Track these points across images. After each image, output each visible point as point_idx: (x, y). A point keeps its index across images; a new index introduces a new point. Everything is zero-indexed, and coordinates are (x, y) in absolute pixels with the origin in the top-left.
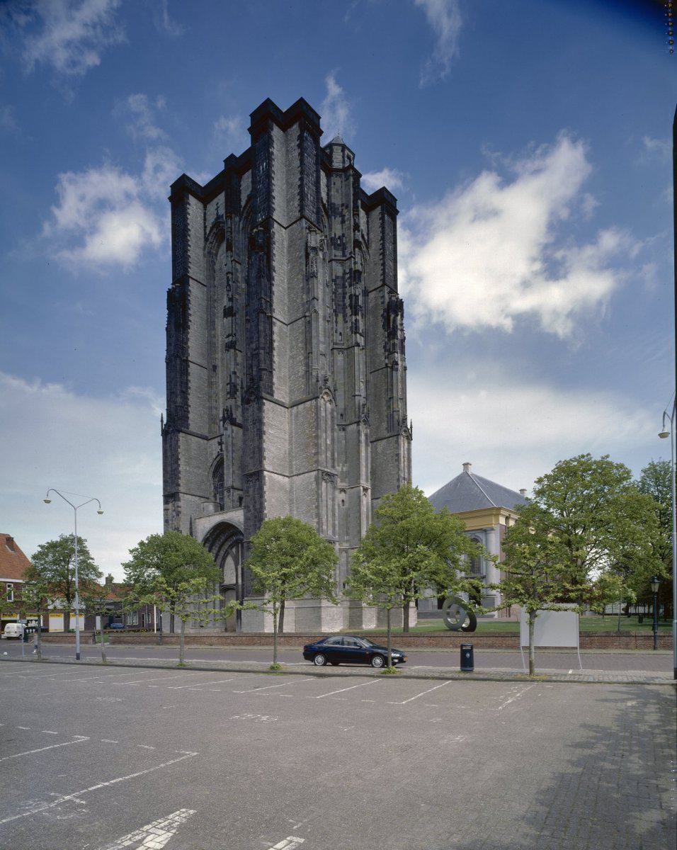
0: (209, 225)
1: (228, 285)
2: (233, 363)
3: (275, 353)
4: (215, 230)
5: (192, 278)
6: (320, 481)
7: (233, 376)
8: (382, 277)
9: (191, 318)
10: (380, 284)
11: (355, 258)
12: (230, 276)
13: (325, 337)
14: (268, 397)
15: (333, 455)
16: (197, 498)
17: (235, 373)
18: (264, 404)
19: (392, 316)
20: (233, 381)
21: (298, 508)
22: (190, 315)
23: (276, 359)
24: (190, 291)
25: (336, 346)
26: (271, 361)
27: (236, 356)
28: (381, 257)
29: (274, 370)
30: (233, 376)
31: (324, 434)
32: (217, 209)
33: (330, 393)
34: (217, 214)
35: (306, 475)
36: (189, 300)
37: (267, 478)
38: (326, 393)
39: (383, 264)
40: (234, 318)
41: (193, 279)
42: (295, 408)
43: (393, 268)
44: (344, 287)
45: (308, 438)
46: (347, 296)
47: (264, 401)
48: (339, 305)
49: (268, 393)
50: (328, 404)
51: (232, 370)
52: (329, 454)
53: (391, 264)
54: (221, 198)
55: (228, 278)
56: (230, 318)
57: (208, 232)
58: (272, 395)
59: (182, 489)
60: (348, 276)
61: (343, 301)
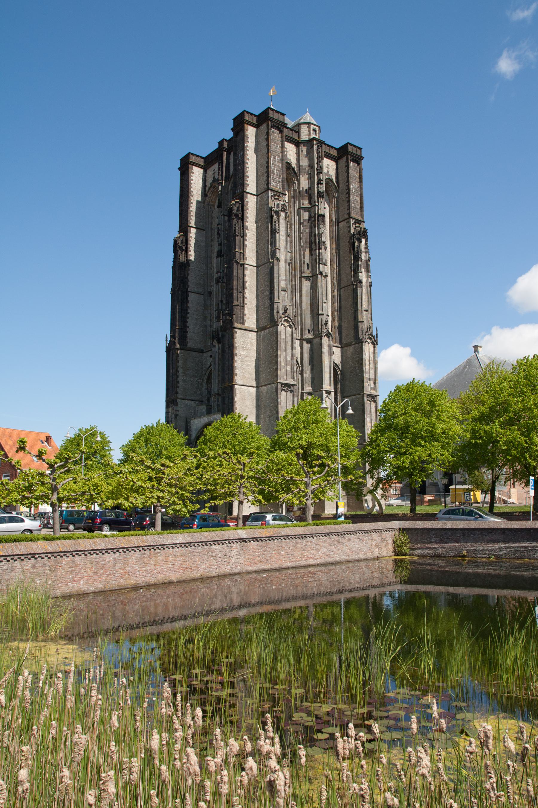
0: (208, 184)
1: (218, 233)
2: (220, 294)
3: (246, 291)
4: (212, 189)
6: (279, 391)
7: (220, 304)
8: (348, 212)
10: (347, 216)
11: (318, 206)
12: (220, 226)
13: (286, 275)
14: (239, 326)
15: (292, 368)
16: (193, 402)
17: (222, 301)
18: (236, 332)
19: (357, 244)
20: (220, 308)
21: (264, 413)
26: (244, 297)
27: (222, 287)
28: (347, 196)
29: (246, 304)
30: (220, 304)
31: (284, 353)
32: (214, 174)
33: (289, 320)
34: (214, 177)
35: (270, 386)
37: (237, 391)
38: (285, 321)
39: (349, 201)
40: (222, 258)
42: (263, 332)
43: (359, 201)
45: (271, 357)
46: (313, 235)
47: (236, 330)
48: (306, 242)
49: (240, 323)
50: (288, 329)
51: (220, 299)
52: (289, 368)
53: (358, 199)
54: (216, 166)
55: (218, 228)
56: (219, 259)
57: (207, 189)
58: (243, 324)
59: (179, 396)
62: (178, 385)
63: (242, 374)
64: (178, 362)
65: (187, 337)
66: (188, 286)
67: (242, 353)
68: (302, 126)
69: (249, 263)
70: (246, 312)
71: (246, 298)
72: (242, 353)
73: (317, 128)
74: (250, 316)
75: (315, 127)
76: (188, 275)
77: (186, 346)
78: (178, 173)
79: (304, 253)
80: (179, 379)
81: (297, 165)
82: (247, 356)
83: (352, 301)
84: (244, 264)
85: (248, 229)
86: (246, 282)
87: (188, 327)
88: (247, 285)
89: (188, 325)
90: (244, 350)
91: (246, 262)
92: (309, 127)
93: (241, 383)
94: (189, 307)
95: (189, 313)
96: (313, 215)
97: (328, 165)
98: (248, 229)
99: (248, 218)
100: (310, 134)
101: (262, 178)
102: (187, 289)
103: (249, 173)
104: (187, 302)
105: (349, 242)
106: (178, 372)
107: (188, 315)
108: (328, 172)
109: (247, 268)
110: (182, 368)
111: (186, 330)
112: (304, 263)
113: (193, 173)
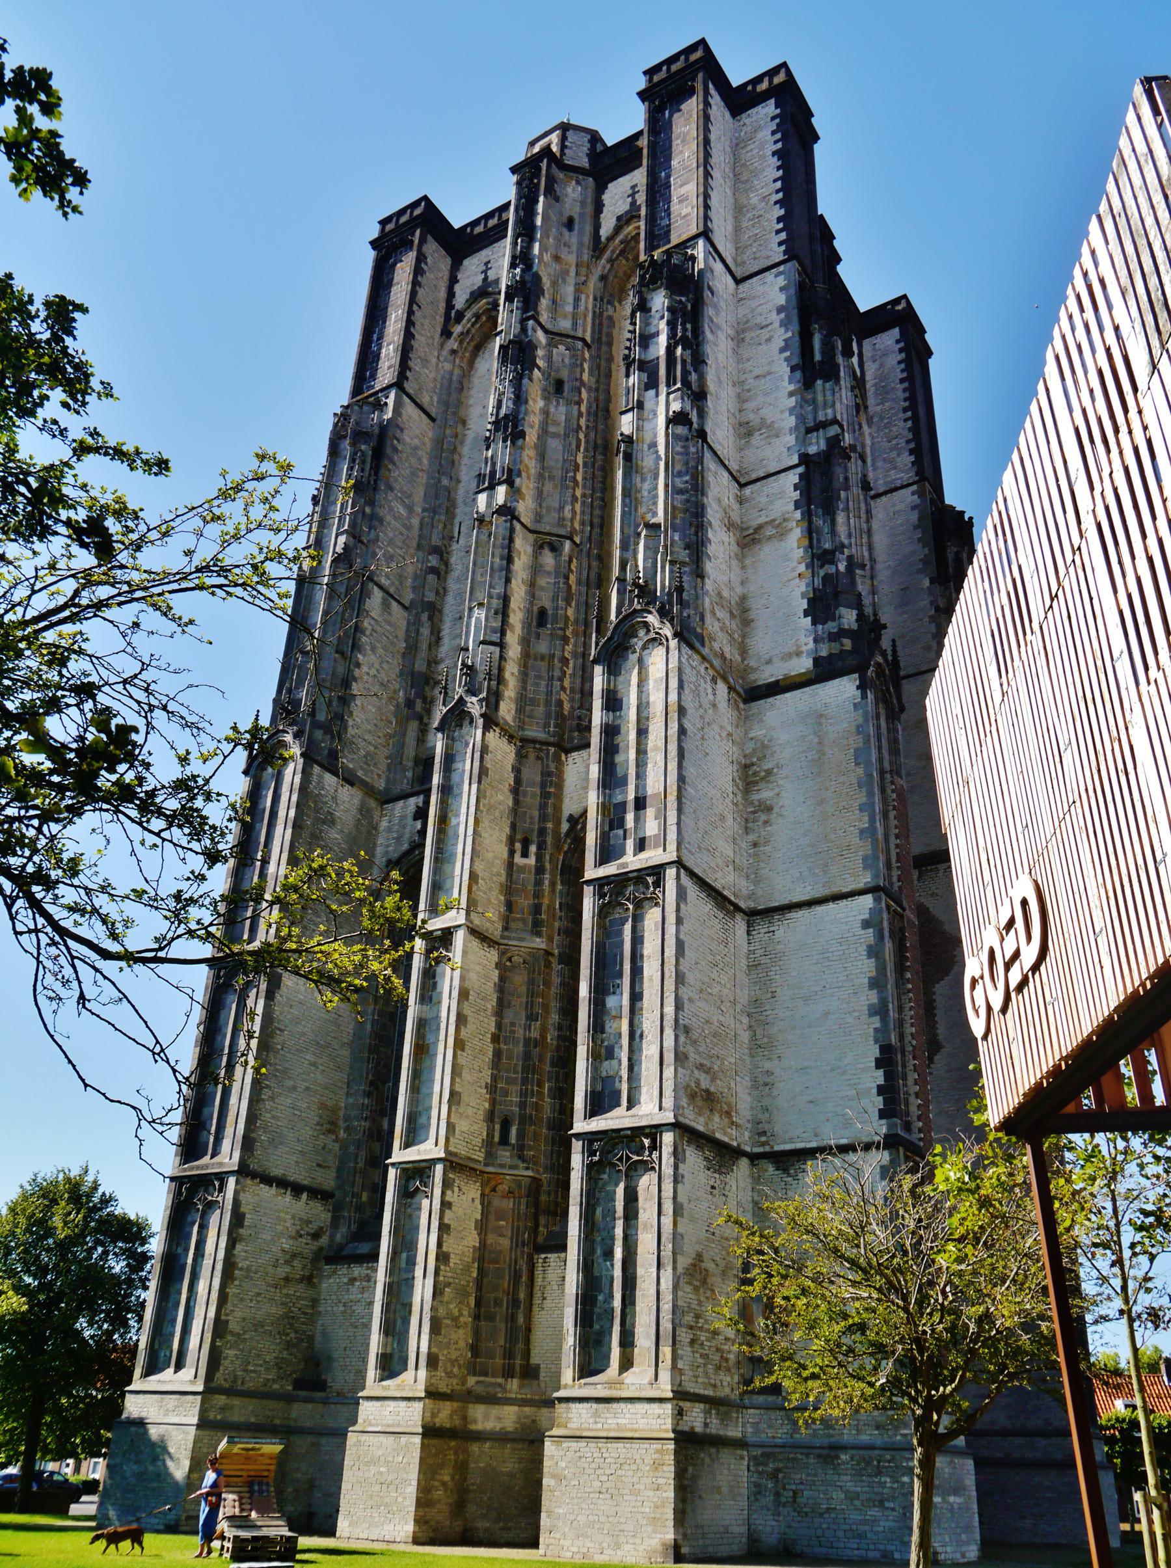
75: (546, 140)
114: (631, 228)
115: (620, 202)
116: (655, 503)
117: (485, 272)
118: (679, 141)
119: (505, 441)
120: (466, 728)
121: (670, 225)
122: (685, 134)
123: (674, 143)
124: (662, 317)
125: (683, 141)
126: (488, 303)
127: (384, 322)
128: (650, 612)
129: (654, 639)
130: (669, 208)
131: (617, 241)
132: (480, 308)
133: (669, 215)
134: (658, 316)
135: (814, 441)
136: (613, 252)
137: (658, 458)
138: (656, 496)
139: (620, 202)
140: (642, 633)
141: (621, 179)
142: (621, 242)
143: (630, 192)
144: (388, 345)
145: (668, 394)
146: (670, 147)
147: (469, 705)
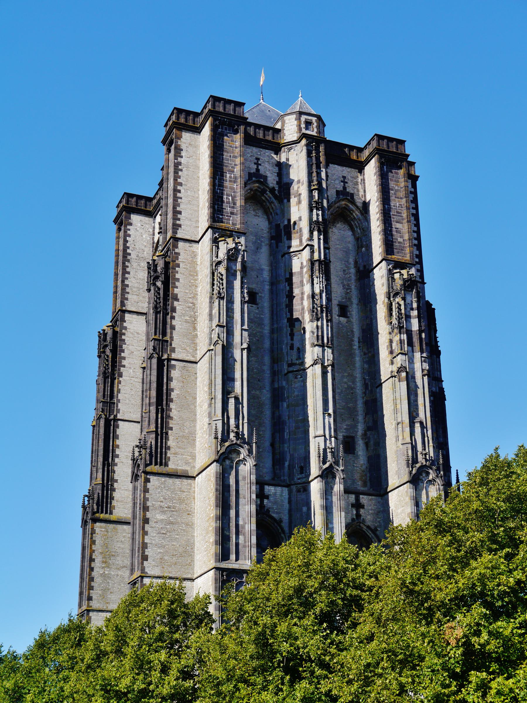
3: (172, 405)
5: (130, 312)
9: (124, 362)
22: (124, 358)
23: (174, 413)
24: (126, 328)
25: (291, 369)
29: (171, 429)
36: (124, 340)
41: (130, 312)
44: (302, 285)
46: (305, 297)
58: (166, 465)
60: (305, 270)
61: (302, 303)
62: (93, 584)
63: (159, 556)
64: (93, 542)
65: (112, 498)
66: (118, 411)
67: (160, 517)
68: (287, 118)
69: (180, 357)
70: (170, 443)
71: (172, 418)
72: (159, 517)
73: (314, 119)
74: (178, 450)
75: (310, 118)
76: (119, 391)
77: (111, 513)
78: (115, 227)
79: (292, 330)
80: (94, 574)
81: (278, 183)
82: (172, 523)
83: (393, 408)
84: (169, 360)
85: (177, 300)
86: (172, 390)
87: (116, 481)
88: (173, 395)
89: (116, 477)
90: (163, 512)
91: (174, 356)
92: (299, 119)
93: (157, 575)
94: (118, 446)
95: (117, 456)
96: (305, 263)
97: (344, 177)
98: (177, 300)
99: (178, 280)
100: (300, 129)
101: (203, 212)
102: (116, 416)
103: (182, 206)
104: (116, 437)
105: (383, 302)
106: (94, 560)
107: (117, 460)
108: (345, 188)
109: (174, 366)
110: (101, 553)
111: (112, 485)
112: (292, 348)
113: (131, 224)
114: (343, 203)
115: (337, 182)
116: (417, 409)
117: (257, 164)
118: (393, 192)
119: (327, 321)
120: (330, 480)
121: (392, 242)
122: (397, 191)
123: (391, 192)
124: (412, 309)
125: (395, 194)
126: (258, 187)
127: (223, 176)
128: (432, 469)
129: (430, 481)
130: (391, 231)
131: (336, 205)
132: (254, 187)
133: (392, 235)
134: (409, 307)
135: (434, 385)
136: (334, 210)
137: (417, 387)
138: (417, 405)
139: (337, 182)
140: (424, 475)
141: (336, 166)
142: (338, 207)
143: (342, 179)
144: (228, 195)
145: (422, 357)
146: (389, 193)
147: (335, 469)
